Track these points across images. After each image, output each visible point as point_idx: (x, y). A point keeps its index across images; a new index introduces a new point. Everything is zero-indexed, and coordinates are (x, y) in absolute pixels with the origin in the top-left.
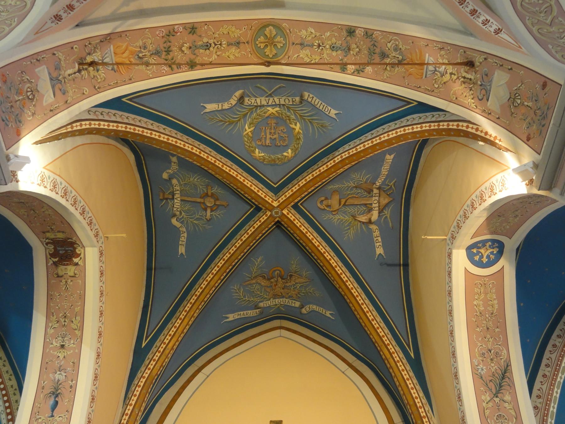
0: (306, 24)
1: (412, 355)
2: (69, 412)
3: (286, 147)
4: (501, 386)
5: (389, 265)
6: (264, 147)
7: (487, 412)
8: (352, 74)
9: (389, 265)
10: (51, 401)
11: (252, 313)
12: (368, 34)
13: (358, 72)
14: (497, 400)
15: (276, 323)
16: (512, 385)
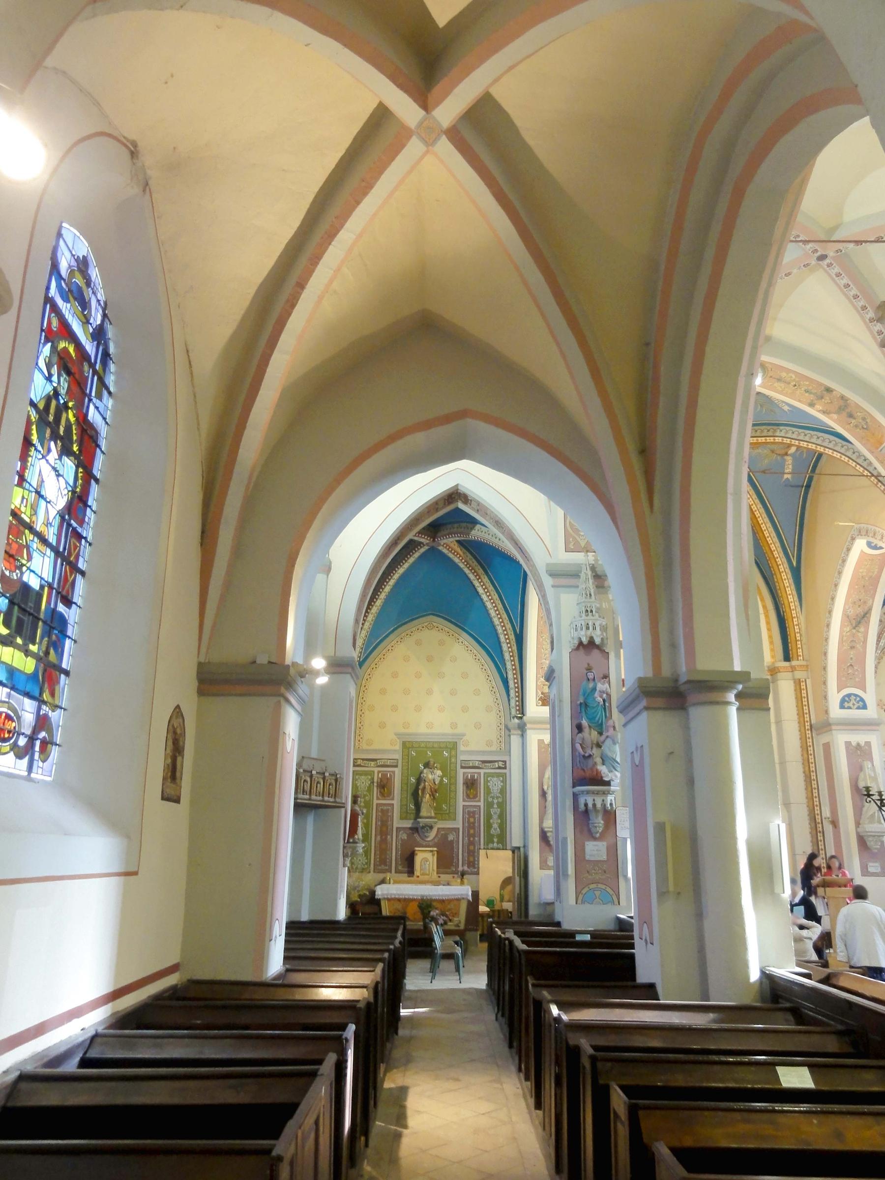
0: (788, 371)
1: (795, 564)
4: (860, 622)
5: (792, 486)
7: (845, 638)
8: (819, 411)
9: (792, 486)
13: (824, 412)
14: (854, 631)
16: (868, 622)
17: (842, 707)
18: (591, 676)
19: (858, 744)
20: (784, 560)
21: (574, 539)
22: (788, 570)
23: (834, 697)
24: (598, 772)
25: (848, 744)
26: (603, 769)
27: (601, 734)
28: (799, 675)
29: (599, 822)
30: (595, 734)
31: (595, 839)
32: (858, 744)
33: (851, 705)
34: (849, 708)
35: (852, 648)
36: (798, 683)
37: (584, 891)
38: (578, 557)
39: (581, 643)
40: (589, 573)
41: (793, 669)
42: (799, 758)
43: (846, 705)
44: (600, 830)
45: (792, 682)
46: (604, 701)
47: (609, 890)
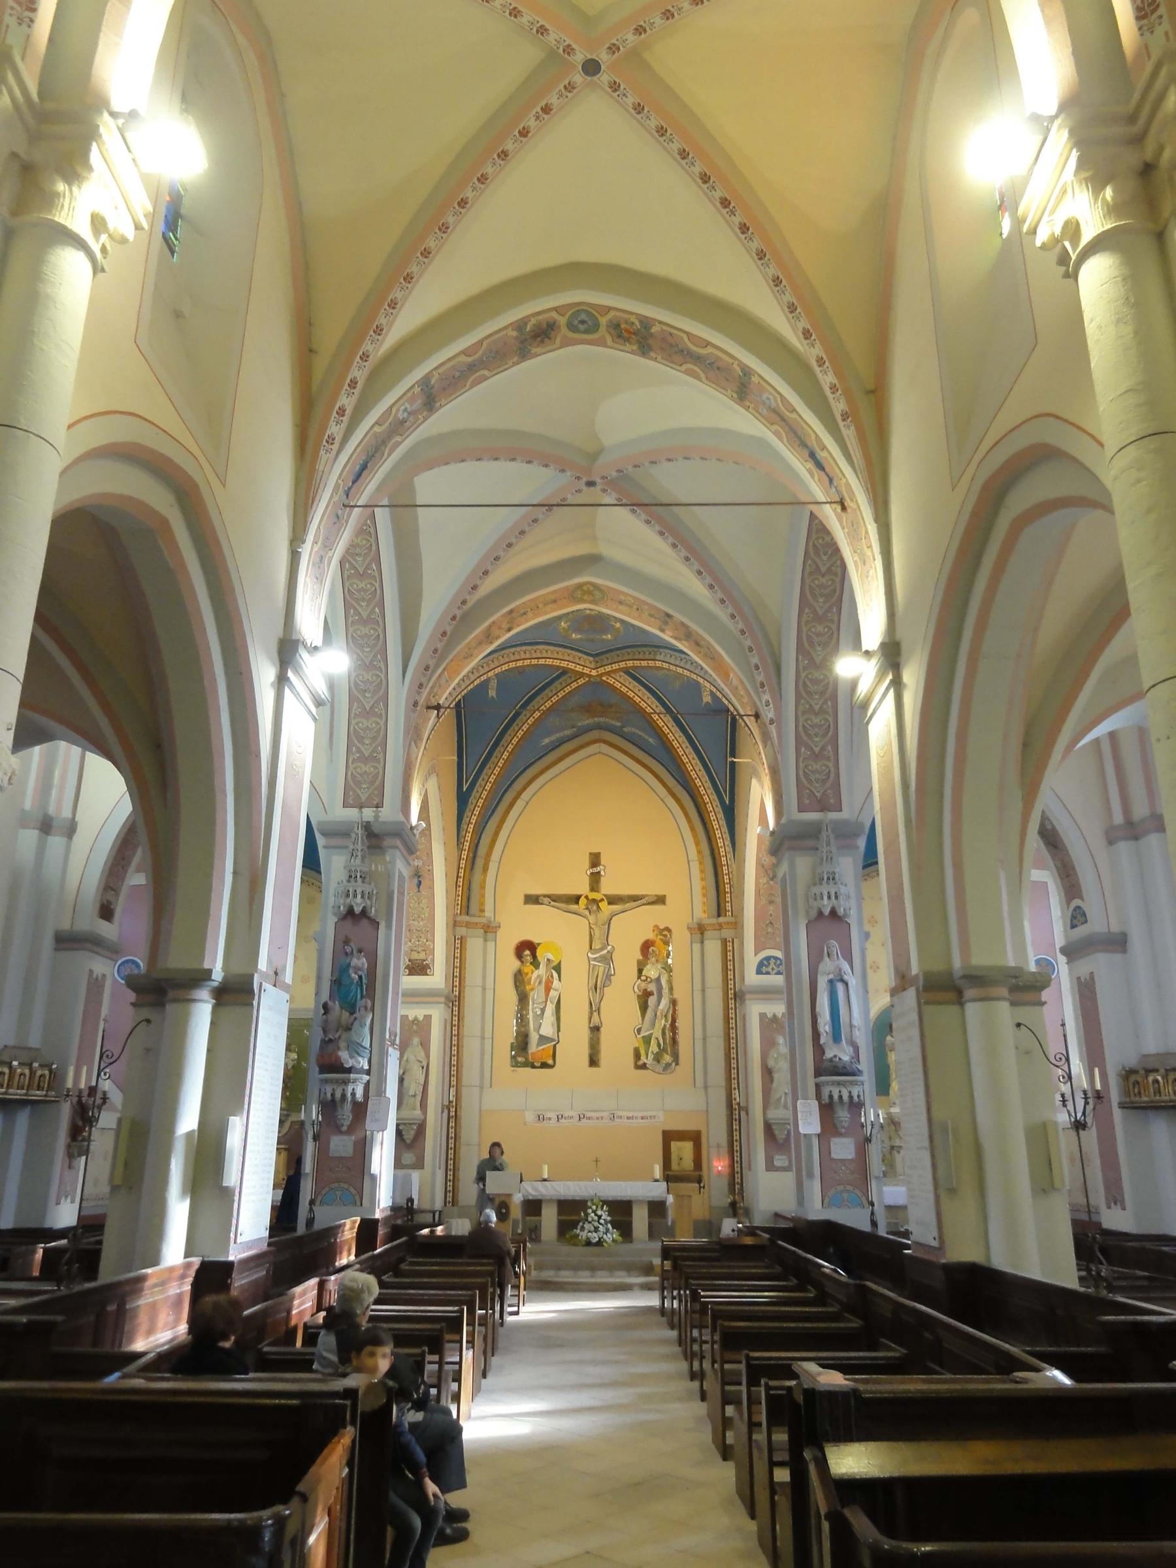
0: (626, 594)
2: (432, 888)
3: (606, 633)
6: (578, 630)
10: (416, 881)
11: (568, 732)
12: (683, 624)
15: (595, 734)
17: (759, 972)
18: (348, 950)
19: (774, 1016)
20: (714, 797)
21: (355, 791)
22: (719, 809)
23: (751, 960)
24: (338, 1058)
25: (762, 1016)
26: (344, 1055)
27: (351, 1014)
28: (727, 933)
29: (346, 1114)
30: (345, 1015)
31: (341, 1133)
32: (774, 1016)
33: (769, 969)
34: (768, 973)
35: (771, 902)
36: (724, 942)
37: (323, 1192)
38: (352, 814)
39: (350, 912)
40: (360, 832)
41: (720, 927)
42: (722, 1034)
43: (764, 969)
44: (347, 1123)
45: (719, 942)
46: (360, 977)
47: (352, 1189)
